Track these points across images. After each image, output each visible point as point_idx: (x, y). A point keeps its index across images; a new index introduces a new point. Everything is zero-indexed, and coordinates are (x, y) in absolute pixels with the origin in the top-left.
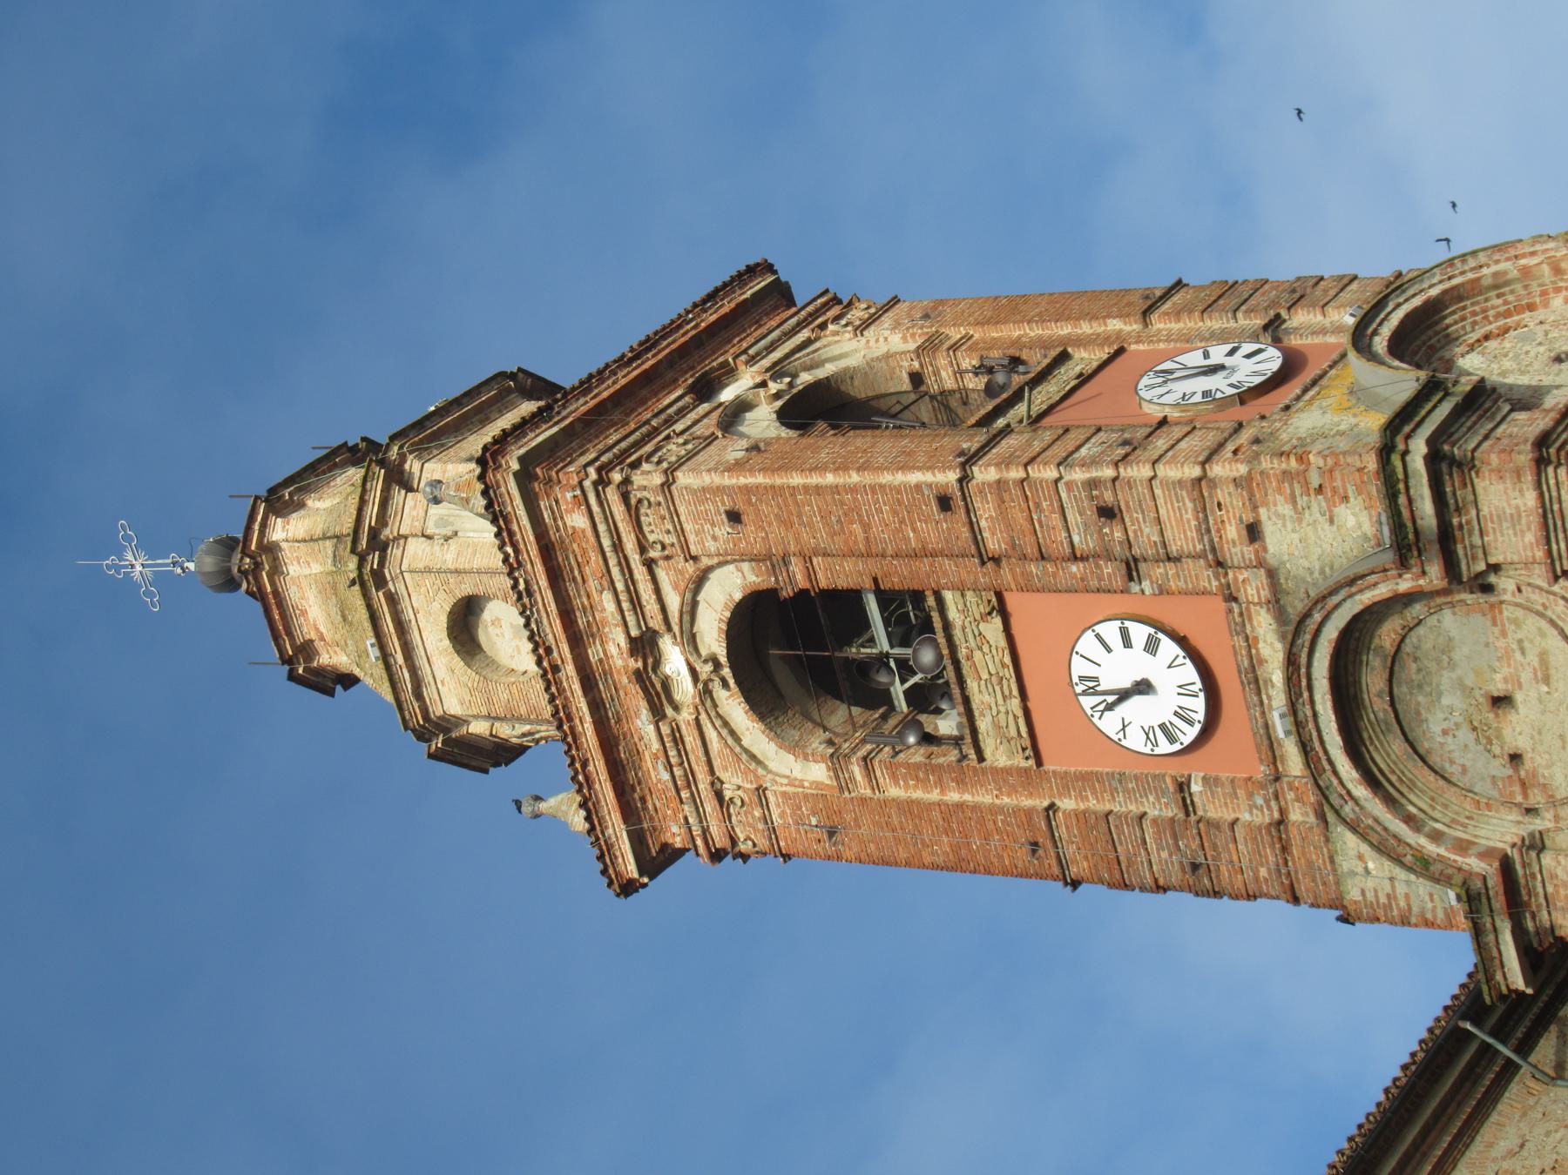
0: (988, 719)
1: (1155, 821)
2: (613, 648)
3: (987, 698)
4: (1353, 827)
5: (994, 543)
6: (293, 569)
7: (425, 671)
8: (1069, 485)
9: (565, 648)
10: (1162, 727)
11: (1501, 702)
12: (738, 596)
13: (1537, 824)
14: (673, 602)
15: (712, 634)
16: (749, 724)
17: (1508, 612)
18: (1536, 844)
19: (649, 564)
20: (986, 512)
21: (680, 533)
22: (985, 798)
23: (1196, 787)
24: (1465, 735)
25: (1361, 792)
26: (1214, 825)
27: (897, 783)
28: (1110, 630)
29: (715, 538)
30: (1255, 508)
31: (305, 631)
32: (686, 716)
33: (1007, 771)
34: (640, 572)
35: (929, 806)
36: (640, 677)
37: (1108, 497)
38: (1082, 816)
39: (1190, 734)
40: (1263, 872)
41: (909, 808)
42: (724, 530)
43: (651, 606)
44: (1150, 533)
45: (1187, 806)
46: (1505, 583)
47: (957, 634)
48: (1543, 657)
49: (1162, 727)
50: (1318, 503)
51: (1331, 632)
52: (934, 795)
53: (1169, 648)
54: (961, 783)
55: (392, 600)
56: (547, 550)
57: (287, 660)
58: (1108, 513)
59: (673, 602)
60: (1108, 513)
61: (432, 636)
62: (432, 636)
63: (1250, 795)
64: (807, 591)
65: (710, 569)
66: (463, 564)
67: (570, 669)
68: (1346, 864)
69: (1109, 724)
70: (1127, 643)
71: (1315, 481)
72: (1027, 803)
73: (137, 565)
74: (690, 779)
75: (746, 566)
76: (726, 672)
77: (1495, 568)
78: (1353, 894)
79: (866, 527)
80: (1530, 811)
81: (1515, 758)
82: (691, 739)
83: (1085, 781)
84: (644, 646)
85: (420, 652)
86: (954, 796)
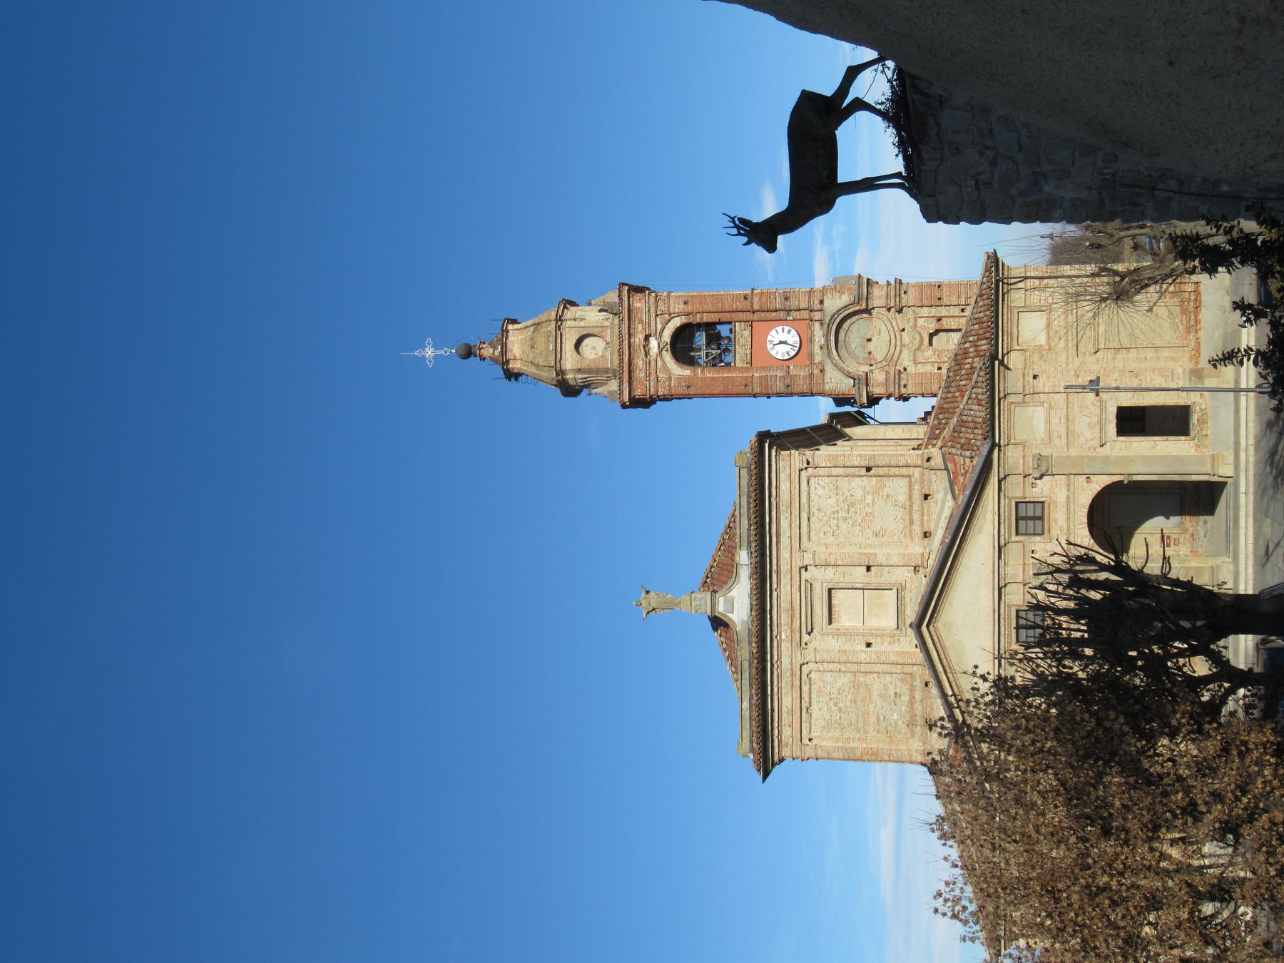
0: (739, 355)
1: (780, 376)
2: (639, 339)
3: (740, 350)
4: (835, 365)
6: (510, 338)
7: (563, 355)
8: (779, 293)
9: (627, 336)
10: (787, 352)
11: (869, 340)
12: (678, 325)
14: (659, 327)
15: (667, 337)
16: (671, 361)
17: (874, 319)
18: (872, 371)
19: (657, 316)
20: (756, 299)
21: (669, 307)
24: (860, 348)
25: (837, 358)
26: (796, 375)
27: (710, 373)
28: (779, 329)
29: (679, 308)
30: (823, 296)
31: (510, 356)
33: (742, 367)
35: (719, 377)
36: (644, 346)
37: (788, 295)
40: (805, 386)
41: (712, 379)
42: (682, 306)
44: (797, 303)
45: (789, 372)
46: (874, 312)
47: (737, 334)
48: (880, 330)
49: (787, 352)
50: (838, 294)
51: (838, 320)
52: (721, 375)
53: (793, 332)
54: (729, 372)
55: (561, 333)
56: (629, 311)
57: (503, 363)
58: (786, 299)
59: (659, 327)
61: (569, 346)
62: (569, 346)
63: (804, 369)
64: (699, 323)
65: (674, 317)
66: (586, 325)
67: (626, 342)
68: (826, 381)
69: (773, 353)
70: (783, 331)
71: (838, 289)
72: (745, 375)
73: (429, 352)
74: (650, 374)
75: (683, 317)
76: (669, 346)
77: (873, 308)
78: (827, 388)
79: (722, 305)
80: (871, 365)
81: (870, 353)
82: (653, 364)
83: (763, 368)
84: (647, 338)
85: (563, 350)
86: (726, 375)
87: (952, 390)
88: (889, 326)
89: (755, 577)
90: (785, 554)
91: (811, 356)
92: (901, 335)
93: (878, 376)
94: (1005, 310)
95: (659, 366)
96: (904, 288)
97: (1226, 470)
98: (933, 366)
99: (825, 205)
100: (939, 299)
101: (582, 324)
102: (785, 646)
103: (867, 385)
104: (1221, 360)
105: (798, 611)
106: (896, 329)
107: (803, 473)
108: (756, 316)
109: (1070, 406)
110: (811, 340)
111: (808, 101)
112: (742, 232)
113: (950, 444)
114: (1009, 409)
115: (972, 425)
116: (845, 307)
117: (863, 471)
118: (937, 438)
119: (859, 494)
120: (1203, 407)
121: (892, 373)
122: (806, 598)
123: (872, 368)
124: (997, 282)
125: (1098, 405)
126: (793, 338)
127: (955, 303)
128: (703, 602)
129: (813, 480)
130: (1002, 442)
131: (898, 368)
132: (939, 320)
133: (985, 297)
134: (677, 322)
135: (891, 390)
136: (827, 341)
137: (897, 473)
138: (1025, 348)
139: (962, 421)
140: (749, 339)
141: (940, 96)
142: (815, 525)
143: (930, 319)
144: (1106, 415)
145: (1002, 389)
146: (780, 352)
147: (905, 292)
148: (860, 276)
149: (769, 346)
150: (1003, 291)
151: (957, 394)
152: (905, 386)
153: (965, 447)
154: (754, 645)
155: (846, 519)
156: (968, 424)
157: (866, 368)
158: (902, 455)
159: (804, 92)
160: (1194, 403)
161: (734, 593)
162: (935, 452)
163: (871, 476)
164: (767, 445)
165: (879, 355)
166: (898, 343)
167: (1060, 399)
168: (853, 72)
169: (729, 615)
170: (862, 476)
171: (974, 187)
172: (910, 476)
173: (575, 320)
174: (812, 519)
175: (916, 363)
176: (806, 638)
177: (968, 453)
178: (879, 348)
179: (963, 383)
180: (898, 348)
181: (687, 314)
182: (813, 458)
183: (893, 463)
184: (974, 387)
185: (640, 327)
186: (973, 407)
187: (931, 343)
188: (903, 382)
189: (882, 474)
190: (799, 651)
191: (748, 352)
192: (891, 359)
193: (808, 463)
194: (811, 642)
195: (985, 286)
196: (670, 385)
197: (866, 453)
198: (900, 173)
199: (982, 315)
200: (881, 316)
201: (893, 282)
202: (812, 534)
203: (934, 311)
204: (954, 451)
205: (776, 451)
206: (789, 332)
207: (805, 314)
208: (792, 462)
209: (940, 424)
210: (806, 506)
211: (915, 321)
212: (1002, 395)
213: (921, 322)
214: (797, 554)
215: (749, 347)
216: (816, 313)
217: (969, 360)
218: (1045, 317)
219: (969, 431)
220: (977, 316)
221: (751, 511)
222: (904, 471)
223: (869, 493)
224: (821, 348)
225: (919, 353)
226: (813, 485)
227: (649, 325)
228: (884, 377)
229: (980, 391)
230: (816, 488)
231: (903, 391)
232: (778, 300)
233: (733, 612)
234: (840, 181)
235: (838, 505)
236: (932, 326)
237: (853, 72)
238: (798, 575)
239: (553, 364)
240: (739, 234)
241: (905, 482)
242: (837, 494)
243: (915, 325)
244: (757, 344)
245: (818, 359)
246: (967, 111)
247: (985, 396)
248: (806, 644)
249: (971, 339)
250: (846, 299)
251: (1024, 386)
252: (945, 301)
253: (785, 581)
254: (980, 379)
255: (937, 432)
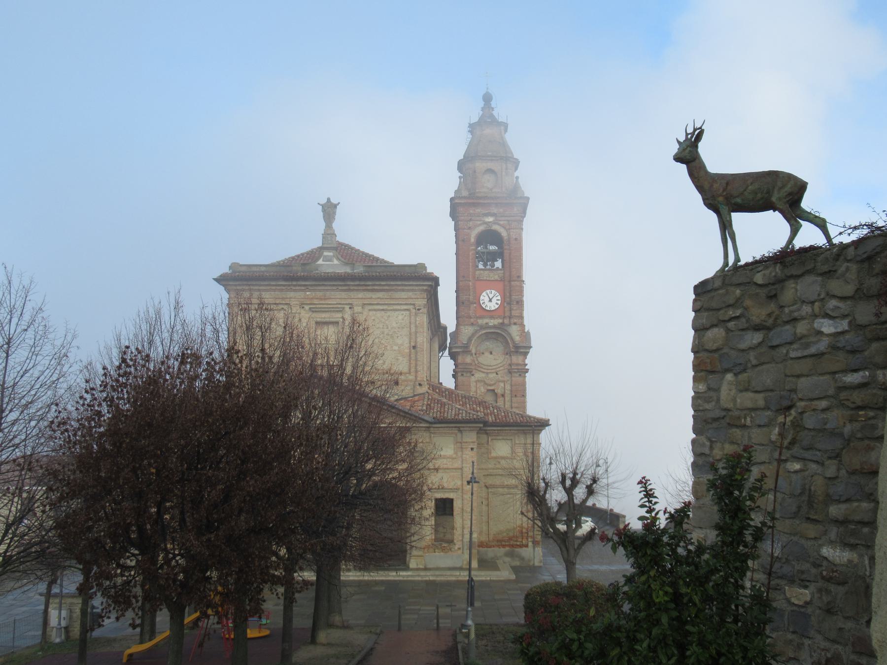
1: (469, 298)
5: (513, 283)
13: (474, 355)
14: (502, 223)
15: (495, 227)
17: (504, 356)
19: (508, 221)
20: (518, 283)
21: (514, 229)
22: (471, 269)
23: (475, 305)
25: (480, 333)
32: (482, 219)
34: (506, 218)
38: (469, 286)
39: (484, 306)
43: (500, 219)
50: (519, 334)
51: (503, 334)
53: (497, 306)
60: (518, 302)
68: (466, 327)
69: (484, 294)
77: (510, 356)
78: (462, 327)
80: (476, 354)
81: (483, 353)
82: (478, 218)
86: (471, 264)
87: (464, 400)
88: (499, 365)
89: (346, 275)
90: (361, 295)
91: (481, 317)
92: (492, 373)
93: (468, 359)
94: (513, 432)
95: (477, 222)
96: (523, 375)
97: (413, 564)
98: (474, 392)
99: (711, 203)
100: (516, 396)
101: (504, 173)
102: (300, 295)
103: (463, 352)
104: (646, 488)
105: (324, 303)
106: (498, 370)
107: (411, 307)
108: (507, 283)
109: (454, 471)
110: (492, 317)
111: (800, 187)
112: (689, 136)
113: (430, 397)
114: (452, 433)
115: (443, 410)
116: (512, 339)
117: (413, 344)
118: (433, 390)
119: (399, 341)
120: (453, 550)
121: (471, 367)
122: (333, 308)
123: (474, 355)
124: (531, 426)
125: (455, 487)
126: (493, 306)
127: (513, 405)
128: (329, 242)
129: (408, 313)
130: (432, 429)
131: (474, 371)
132: (503, 396)
133: (521, 419)
134: (504, 234)
135: (460, 367)
136: (491, 327)
137: (412, 365)
138: (490, 443)
139: (445, 405)
140: (493, 279)
141: (835, 271)
142: (379, 314)
143: (503, 390)
144: (448, 492)
145: (465, 429)
146: (484, 298)
147: (520, 375)
148: (531, 347)
149: (488, 291)
150: (527, 430)
151: (461, 403)
152: (462, 375)
153: (428, 407)
154: (302, 274)
155: (383, 333)
156: (443, 408)
157: (473, 351)
158: (423, 368)
159: (807, 183)
160: (455, 544)
161: (336, 262)
162: (424, 389)
163: (410, 349)
164: (430, 283)
165: (481, 359)
166: (489, 371)
167: (457, 464)
168: (821, 224)
169: (322, 259)
170: (410, 343)
171: (733, 315)
172: (410, 373)
173: (507, 169)
174: (383, 312)
175: (477, 381)
176: (307, 307)
177: (425, 408)
178: (487, 359)
179: (468, 406)
180: (485, 371)
181: (509, 240)
182: (422, 313)
183: (419, 363)
184: (466, 412)
185: (501, 210)
186: (454, 411)
187: (488, 390)
188: (465, 374)
189: (412, 356)
190: (298, 303)
191: (485, 278)
192: (480, 367)
193: (419, 310)
194: (305, 310)
195: (528, 419)
196: (464, 229)
197: (425, 346)
198: (739, 261)
199: (511, 417)
200: (506, 360)
201: (527, 367)
202: (374, 312)
203: (508, 392)
204: (426, 400)
205: (426, 289)
206: (497, 304)
207: (507, 314)
208: (419, 300)
209: (442, 392)
210: (392, 308)
211: (504, 382)
212: (461, 429)
213: (502, 385)
214: (360, 302)
215: (488, 279)
216: (508, 320)
217: (482, 410)
218: (508, 455)
219: (439, 409)
220: (510, 414)
221: (388, 273)
222: (413, 370)
223: (399, 347)
224: (487, 323)
225: (482, 384)
226: (404, 313)
227: (502, 216)
228: (468, 362)
229: (464, 415)
230: (403, 314)
231: (459, 374)
232: (517, 297)
233: (323, 261)
234: (733, 214)
235: (392, 328)
236: (499, 391)
237: (821, 224)
238: (347, 303)
239: (479, 154)
240: (687, 134)
241: (406, 370)
242: (399, 328)
243: (500, 381)
244: (489, 284)
245: (480, 321)
246: (819, 295)
247: (460, 418)
248: (303, 307)
249: (495, 411)
250: (517, 339)
251: (466, 442)
252: (514, 399)
253: (344, 295)
254: (471, 415)
255: (438, 391)
